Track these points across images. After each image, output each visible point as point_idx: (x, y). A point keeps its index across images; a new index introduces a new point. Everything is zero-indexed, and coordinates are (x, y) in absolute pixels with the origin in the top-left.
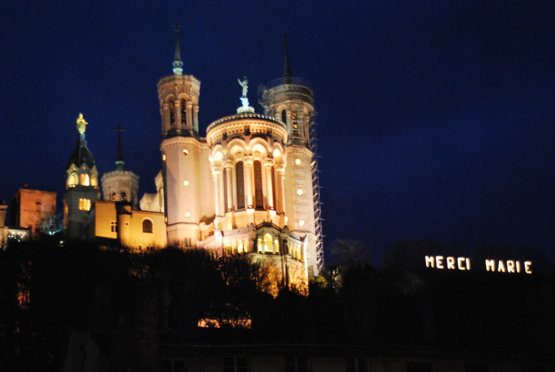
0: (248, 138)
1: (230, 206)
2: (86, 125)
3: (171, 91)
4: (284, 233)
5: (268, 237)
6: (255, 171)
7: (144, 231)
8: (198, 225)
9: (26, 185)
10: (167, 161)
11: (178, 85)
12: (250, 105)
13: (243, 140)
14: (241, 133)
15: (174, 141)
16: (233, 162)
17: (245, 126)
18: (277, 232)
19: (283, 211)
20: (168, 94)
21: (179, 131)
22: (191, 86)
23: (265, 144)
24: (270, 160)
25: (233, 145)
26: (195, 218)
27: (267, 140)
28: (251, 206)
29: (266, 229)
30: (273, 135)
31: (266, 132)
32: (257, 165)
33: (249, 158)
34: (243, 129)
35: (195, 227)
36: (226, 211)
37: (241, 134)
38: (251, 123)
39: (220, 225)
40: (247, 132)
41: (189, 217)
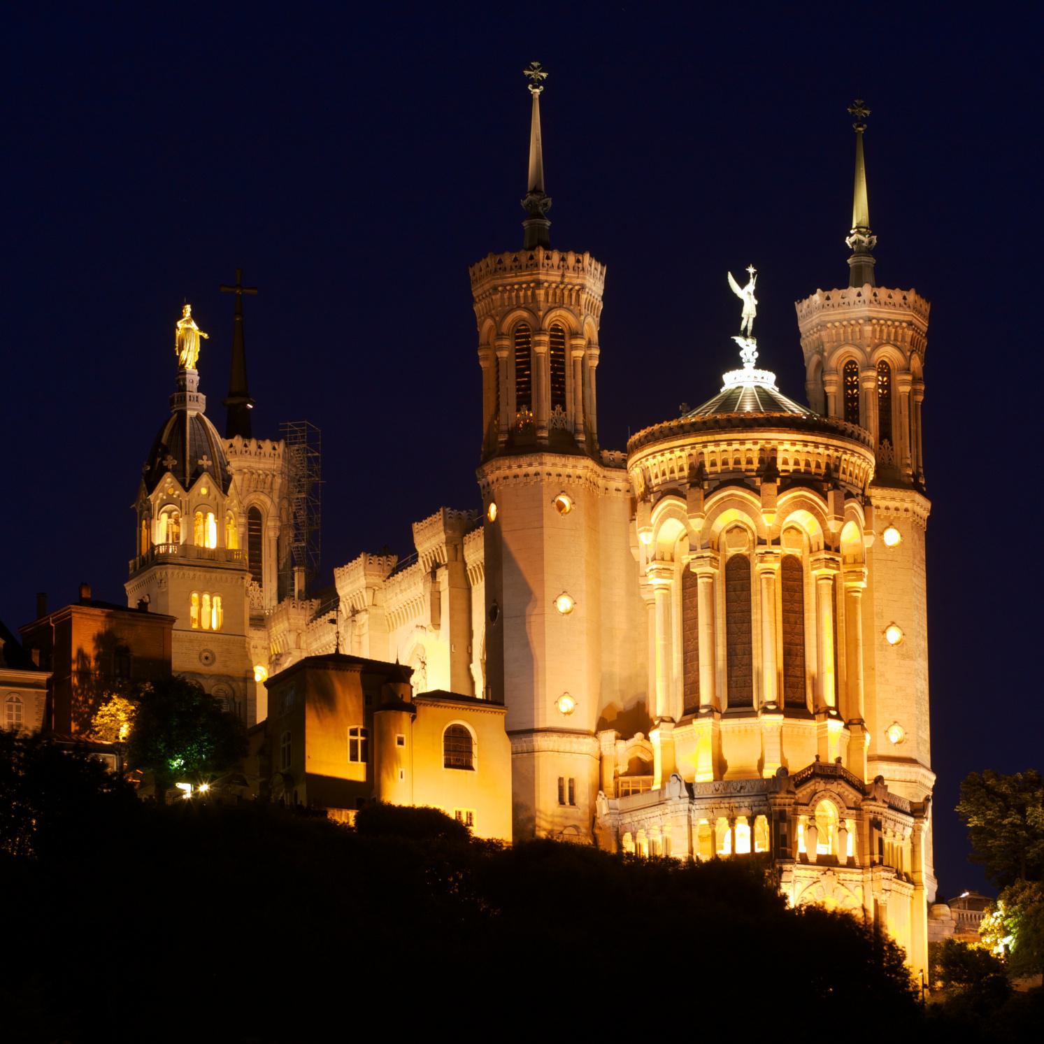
0: (772, 488)
1: (705, 698)
2: (201, 337)
3: (522, 301)
4: (874, 799)
5: (827, 809)
6: (785, 589)
7: (448, 765)
8: (595, 735)
9: (86, 594)
10: (504, 528)
11: (546, 284)
12: (760, 365)
13: (755, 495)
14: (747, 470)
15: (530, 465)
16: (719, 558)
17: (762, 450)
18: (852, 795)
19: (859, 714)
20: (512, 310)
21: (545, 434)
22: (583, 287)
23: (820, 507)
24: (832, 557)
25: (722, 507)
26: (587, 721)
27: (825, 498)
28: (774, 703)
29: (820, 785)
30: (842, 476)
31: (823, 470)
32: (792, 571)
33: (771, 553)
34: (755, 457)
35: (587, 744)
36: (692, 710)
37: (749, 474)
38: (781, 442)
39: (668, 746)
40: (768, 469)
41: (568, 713)
